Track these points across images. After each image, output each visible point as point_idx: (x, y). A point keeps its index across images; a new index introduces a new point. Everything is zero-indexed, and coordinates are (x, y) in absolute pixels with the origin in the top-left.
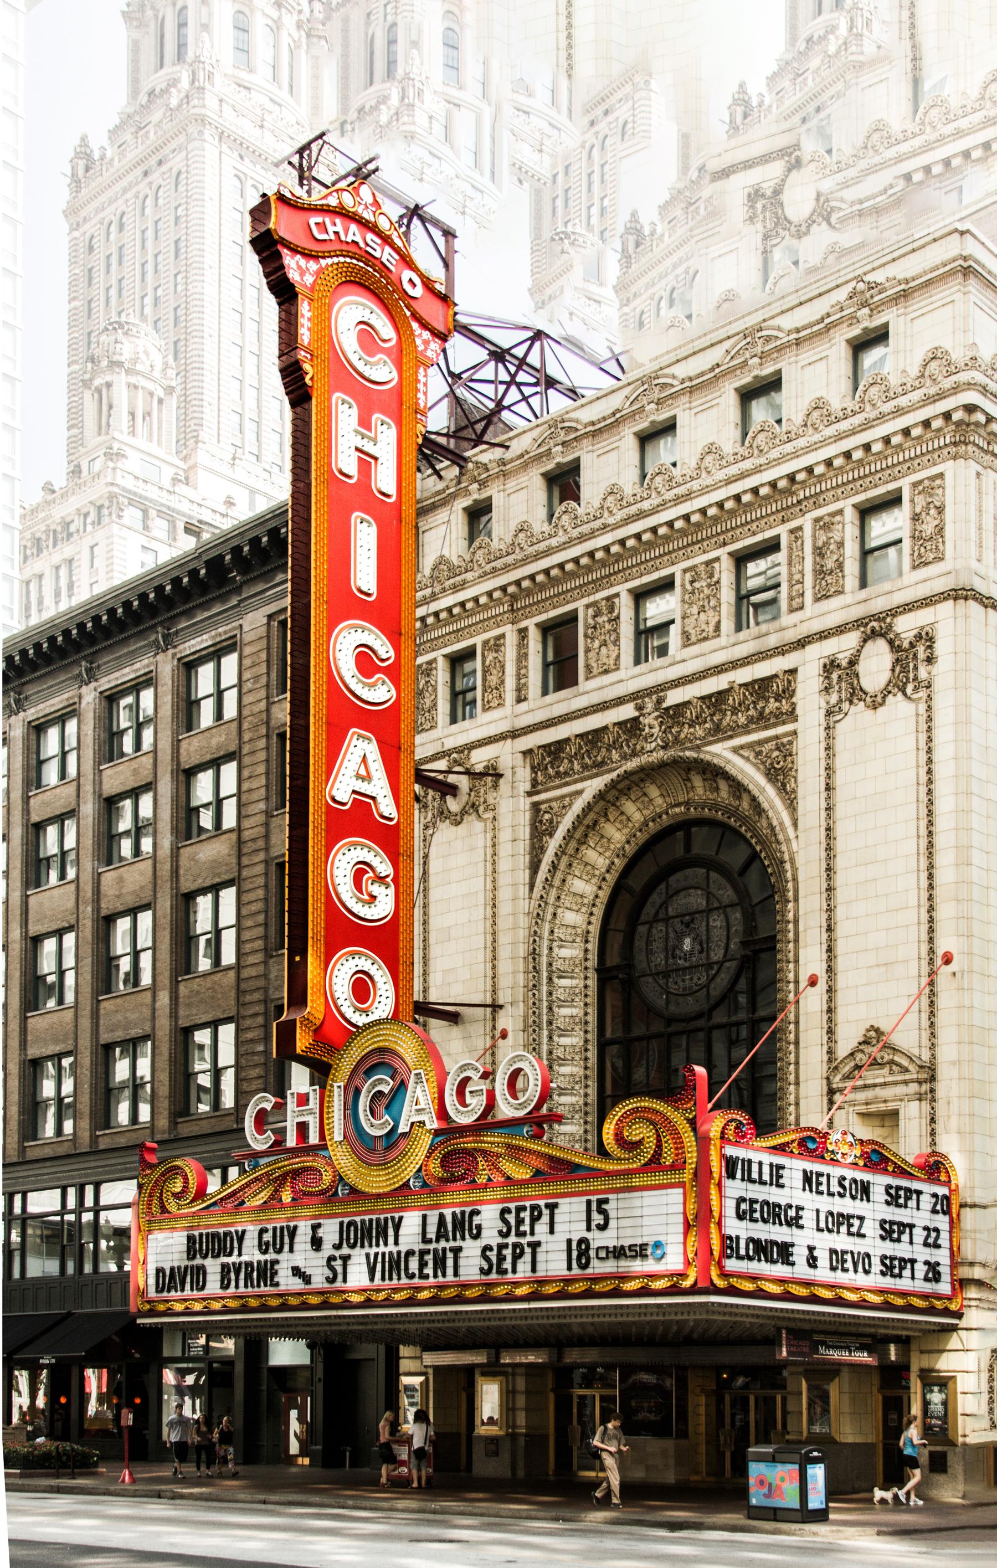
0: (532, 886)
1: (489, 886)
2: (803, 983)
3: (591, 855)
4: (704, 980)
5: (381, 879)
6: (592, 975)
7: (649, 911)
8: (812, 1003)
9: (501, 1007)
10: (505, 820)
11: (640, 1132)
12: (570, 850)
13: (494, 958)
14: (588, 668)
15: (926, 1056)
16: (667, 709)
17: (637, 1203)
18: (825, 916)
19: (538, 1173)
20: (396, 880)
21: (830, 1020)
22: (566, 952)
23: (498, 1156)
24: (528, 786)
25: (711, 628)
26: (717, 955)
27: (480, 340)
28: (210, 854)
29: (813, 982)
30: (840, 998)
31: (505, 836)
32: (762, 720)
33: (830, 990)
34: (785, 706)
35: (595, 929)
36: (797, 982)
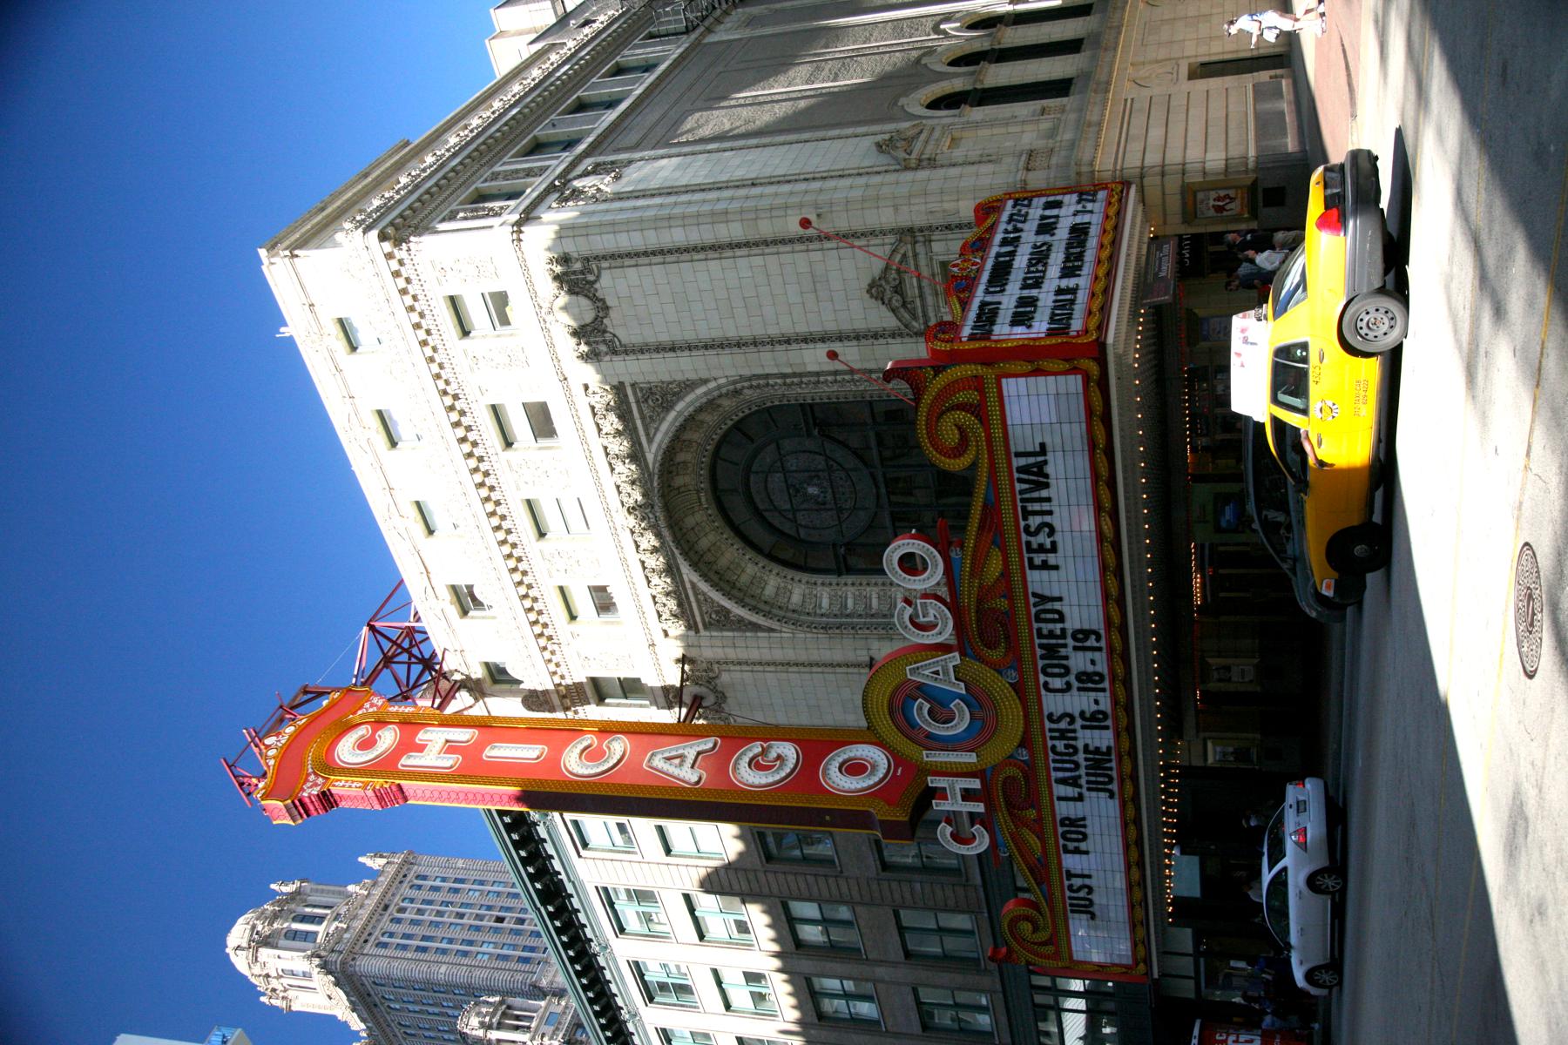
0: (771, 630)
1: (772, 668)
4: (843, 475)
5: (764, 752)
6: (843, 579)
7: (787, 528)
8: (851, 354)
9: (872, 659)
10: (719, 653)
11: (951, 436)
12: (741, 595)
13: (831, 665)
15: (890, 239)
17: (1018, 431)
18: (778, 347)
20: (766, 740)
21: (865, 337)
22: (825, 603)
23: (981, 587)
29: (833, 355)
31: (731, 654)
33: (840, 339)
35: (805, 577)
36: (836, 373)
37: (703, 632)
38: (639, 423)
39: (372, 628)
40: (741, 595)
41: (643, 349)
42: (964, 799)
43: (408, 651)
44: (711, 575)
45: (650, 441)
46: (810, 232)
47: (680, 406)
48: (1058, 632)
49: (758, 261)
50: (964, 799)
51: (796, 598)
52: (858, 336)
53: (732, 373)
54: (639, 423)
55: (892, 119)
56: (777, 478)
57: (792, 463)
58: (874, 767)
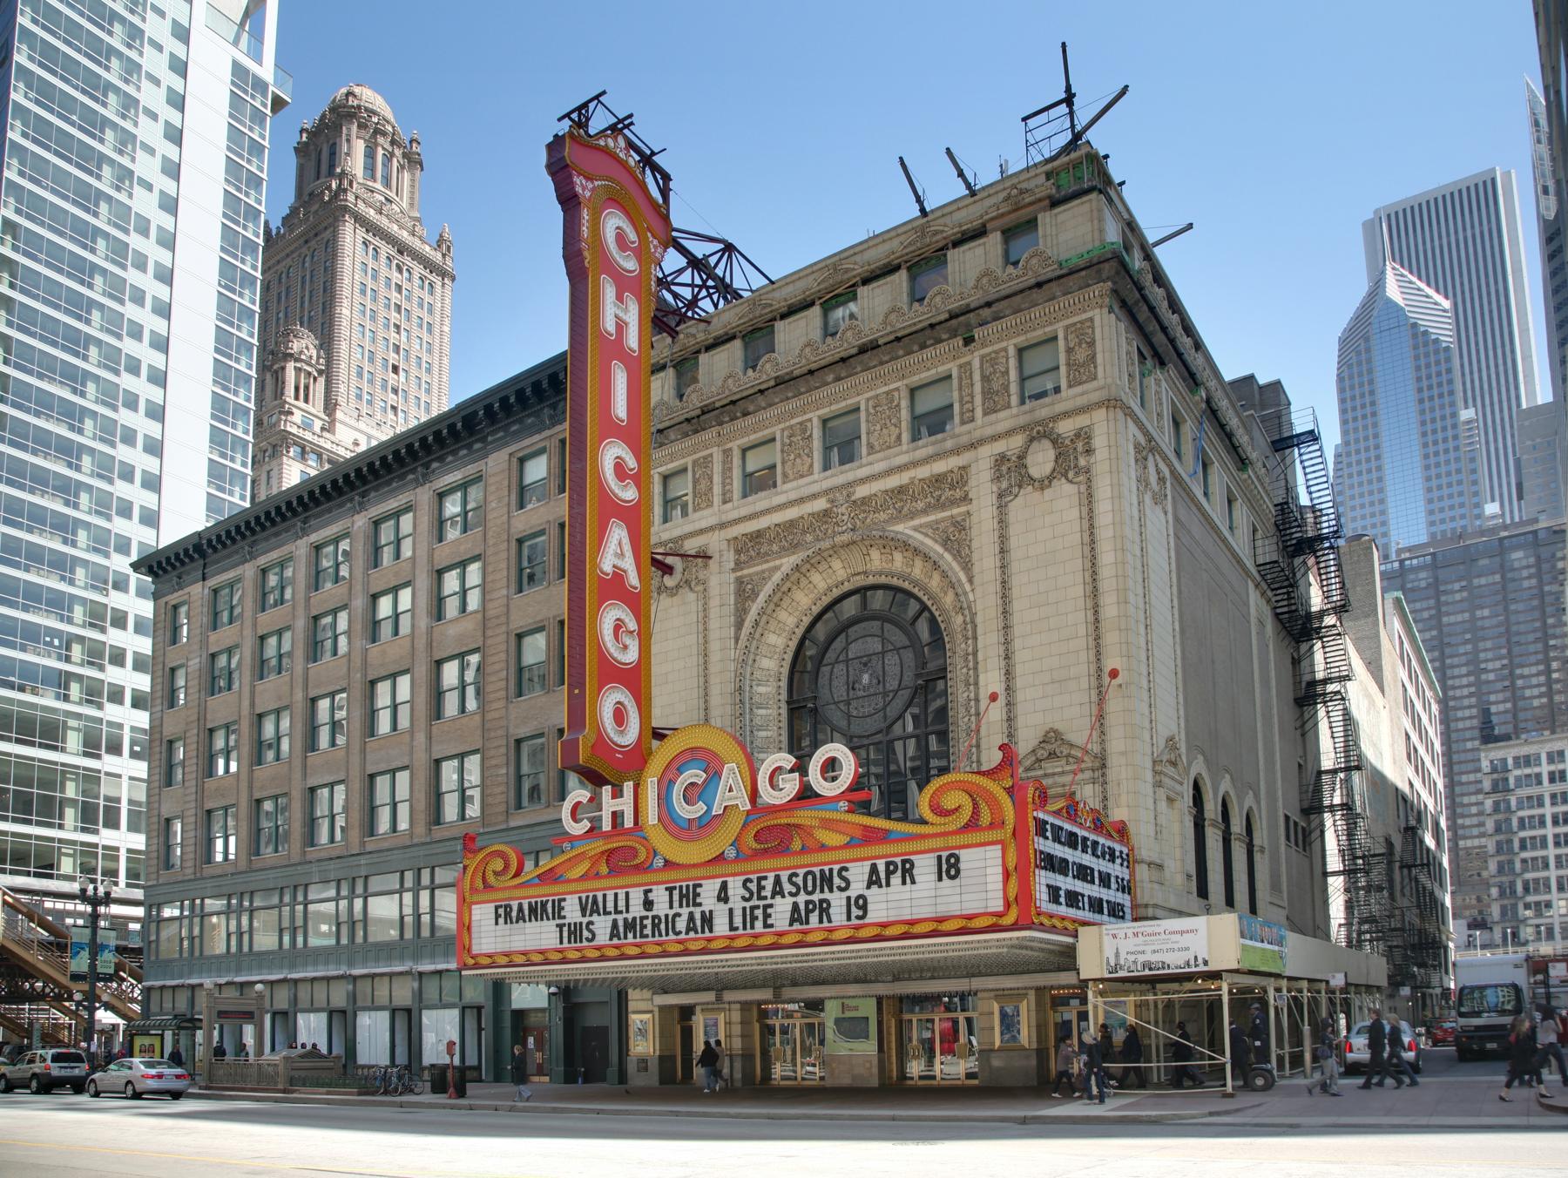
0: (737, 640)
2: (984, 703)
3: (782, 615)
6: (784, 706)
14: (785, 475)
18: (1002, 648)
21: (1010, 726)
22: (762, 689)
24: (732, 565)
25: (893, 438)
26: (892, 684)
27: (683, 251)
28: (456, 629)
29: (994, 697)
30: (1020, 709)
31: (714, 603)
32: (940, 505)
33: (1009, 704)
34: (958, 494)
35: (785, 671)
36: (977, 700)
37: (733, 576)
38: (932, 518)
40: (769, 611)
41: (1003, 523)
42: (614, 814)
43: (704, 286)
44: (788, 584)
45: (915, 529)
46: (1106, 679)
47: (947, 556)
48: (763, 894)
49: (1082, 631)
50: (614, 814)
51: (766, 663)
52: (1010, 719)
53: (979, 607)
54: (932, 518)
55: (1188, 749)
56: (875, 645)
57: (892, 660)
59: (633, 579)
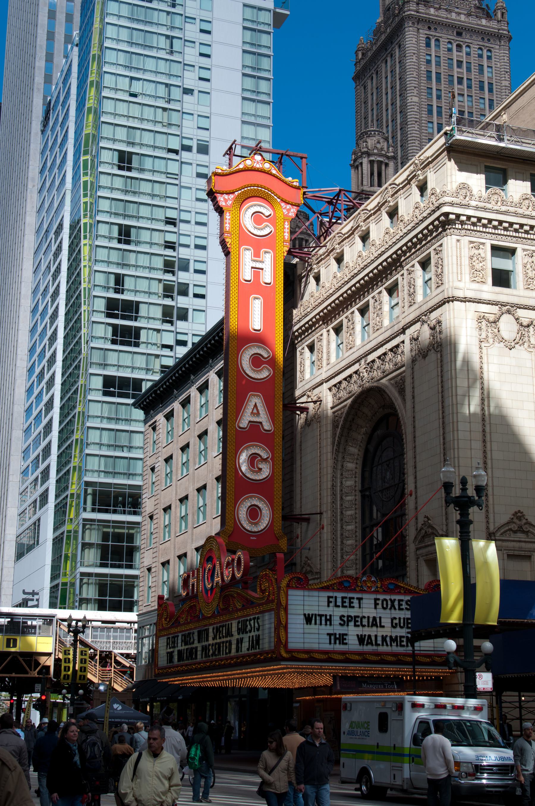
16: (368, 364)
19: (243, 606)
31: (324, 429)
33: (416, 498)
35: (359, 471)
39: (340, 191)
58: (256, 524)
59: (267, 426)
